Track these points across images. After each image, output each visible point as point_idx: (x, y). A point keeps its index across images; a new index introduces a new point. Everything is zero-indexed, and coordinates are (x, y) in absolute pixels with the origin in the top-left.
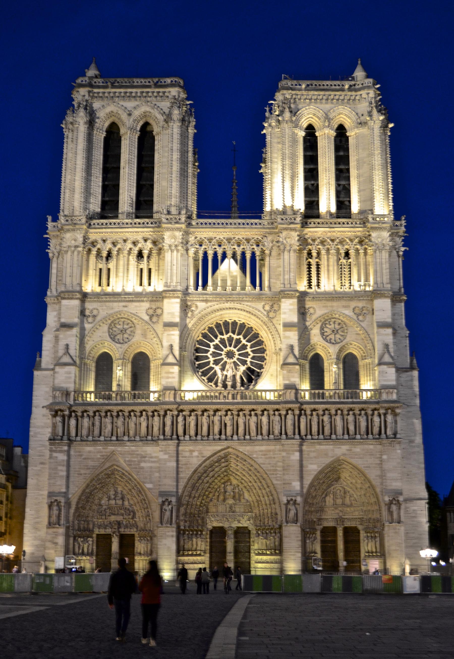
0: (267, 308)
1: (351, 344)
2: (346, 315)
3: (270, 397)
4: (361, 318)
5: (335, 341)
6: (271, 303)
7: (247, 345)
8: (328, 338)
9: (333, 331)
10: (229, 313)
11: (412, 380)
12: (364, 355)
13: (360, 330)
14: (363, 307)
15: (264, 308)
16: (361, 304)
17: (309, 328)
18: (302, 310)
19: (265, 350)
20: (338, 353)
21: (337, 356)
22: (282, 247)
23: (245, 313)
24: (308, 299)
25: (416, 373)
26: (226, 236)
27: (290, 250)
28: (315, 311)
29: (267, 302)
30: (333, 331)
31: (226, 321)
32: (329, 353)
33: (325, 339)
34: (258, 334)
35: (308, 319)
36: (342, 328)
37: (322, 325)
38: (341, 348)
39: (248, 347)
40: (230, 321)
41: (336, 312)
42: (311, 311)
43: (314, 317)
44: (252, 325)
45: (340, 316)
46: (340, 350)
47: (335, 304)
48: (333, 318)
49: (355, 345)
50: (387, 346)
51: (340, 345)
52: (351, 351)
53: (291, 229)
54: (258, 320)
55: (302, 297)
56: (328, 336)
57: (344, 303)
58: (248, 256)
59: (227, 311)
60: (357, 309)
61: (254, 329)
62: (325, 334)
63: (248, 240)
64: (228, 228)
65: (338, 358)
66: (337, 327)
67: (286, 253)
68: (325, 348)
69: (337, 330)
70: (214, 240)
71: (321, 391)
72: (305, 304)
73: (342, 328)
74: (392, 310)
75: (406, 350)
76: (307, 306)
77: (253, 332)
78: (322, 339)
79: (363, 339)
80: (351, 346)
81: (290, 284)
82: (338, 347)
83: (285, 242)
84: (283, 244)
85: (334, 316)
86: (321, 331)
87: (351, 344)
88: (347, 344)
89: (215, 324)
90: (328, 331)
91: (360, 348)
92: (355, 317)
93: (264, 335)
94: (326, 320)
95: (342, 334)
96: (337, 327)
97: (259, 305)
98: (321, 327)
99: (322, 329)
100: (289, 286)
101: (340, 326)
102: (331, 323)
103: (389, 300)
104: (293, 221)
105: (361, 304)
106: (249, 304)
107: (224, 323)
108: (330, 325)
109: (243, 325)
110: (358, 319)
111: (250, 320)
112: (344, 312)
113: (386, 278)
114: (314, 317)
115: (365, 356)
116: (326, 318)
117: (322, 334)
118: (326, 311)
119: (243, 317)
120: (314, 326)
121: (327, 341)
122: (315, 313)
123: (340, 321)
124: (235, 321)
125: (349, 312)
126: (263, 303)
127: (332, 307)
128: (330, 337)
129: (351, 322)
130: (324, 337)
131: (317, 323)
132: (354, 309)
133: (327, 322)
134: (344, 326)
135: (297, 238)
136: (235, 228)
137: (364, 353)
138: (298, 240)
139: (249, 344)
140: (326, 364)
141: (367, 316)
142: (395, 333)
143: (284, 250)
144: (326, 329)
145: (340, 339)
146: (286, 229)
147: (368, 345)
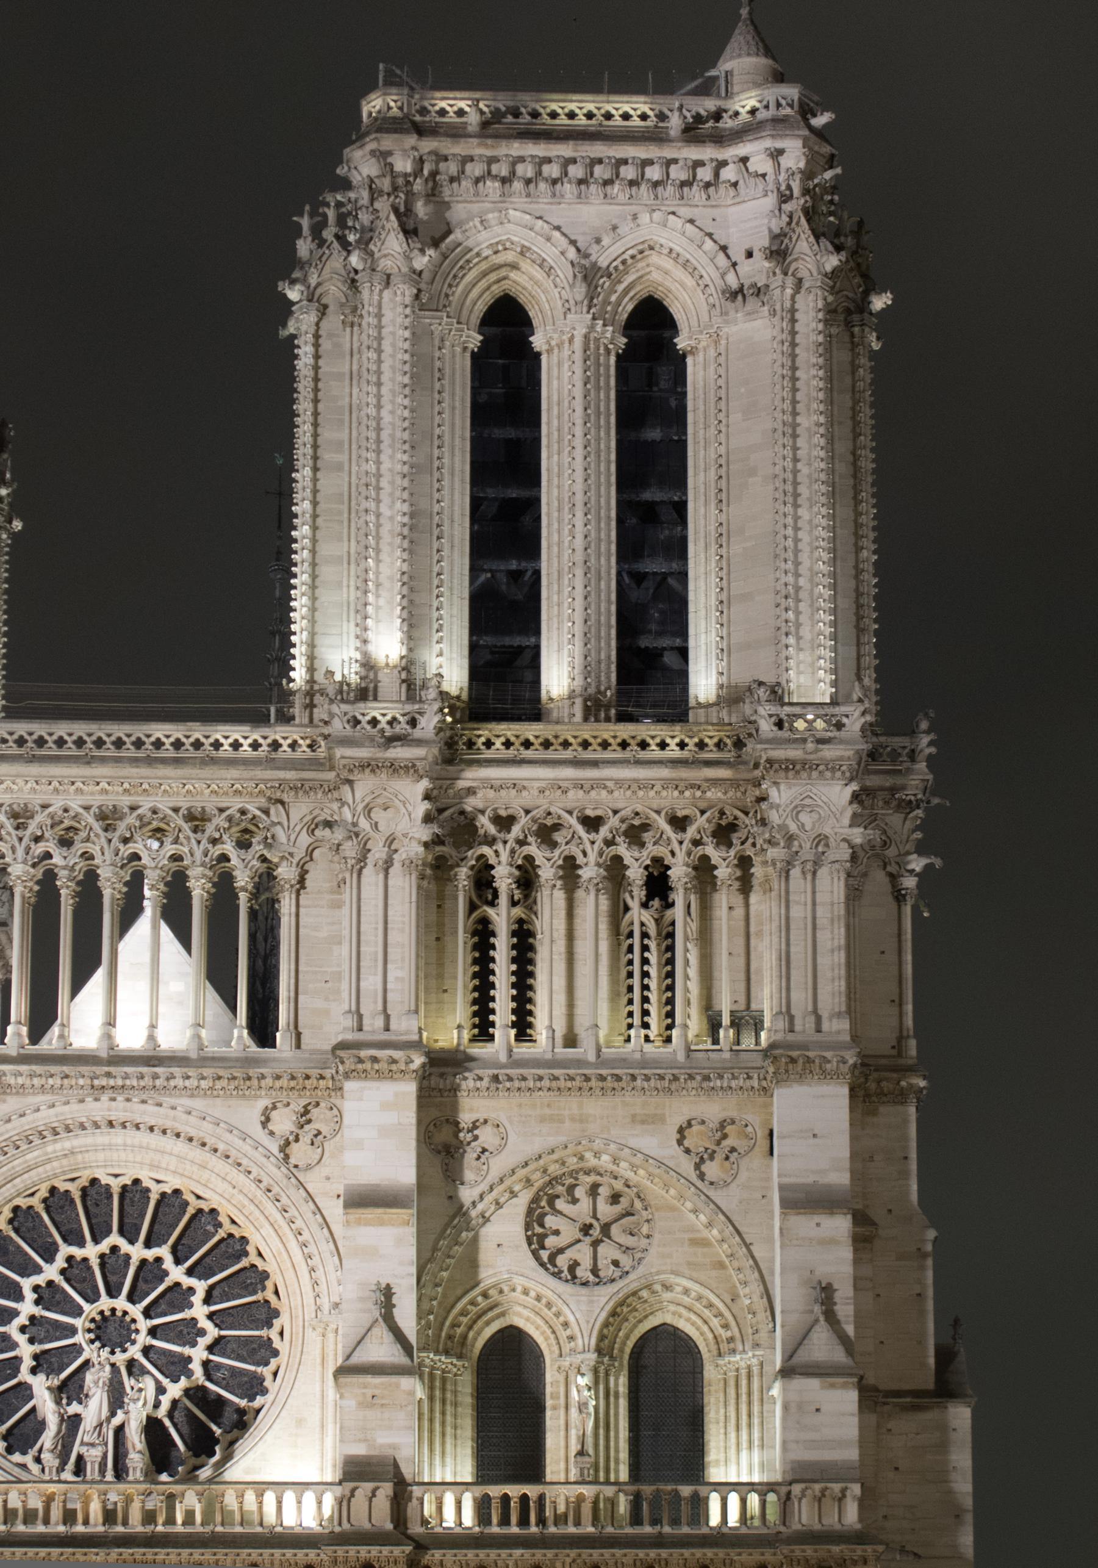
0: (284, 1122)
1: (667, 1287)
2: (647, 1157)
3: (306, 1514)
4: (712, 1169)
5: (595, 1271)
6: (298, 1105)
7: (191, 1290)
8: (562, 1261)
9: (586, 1229)
10: (110, 1147)
11: (943, 1446)
12: (724, 1334)
13: (710, 1225)
14: (722, 1125)
15: (266, 1121)
16: (713, 1109)
17: (473, 1213)
18: (444, 1135)
19: (276, 1314)
20: (606, 1324)
21: (602, 1338)
22: (350, 849)
23: (180, 1146)
24: (471, 1083)
25: (960, 1416)
26: (96, 801)
27: (388, 864)
28: (504, 1138)
29: (283, 1096)
30: (586, 1229)
31: (94, 1181)
32: (565, 1327)
33: (549, 1265)
34: (244, 1240)
35: (469, 1175)
36: (622, 1213)
37: (535, 1200)
38: (622, 1303)
39: (197, 1299)
40: (116, 1185)
41: (598, 1144)
42: (487, 1136)
43: (498, 1165)
44: (213, 1200)
45: (615, 1161)
46: (614, 1314)
47: (594, 1106)
48: (587, 1173)
49: (686, 1292)
50: (826, 1293)
51: (612, 1288)
52: (669, 1319)
53: (395, 768)
54: (241, 1179)
55: (441, 1074)
56: (561, 1251)
57: (635, 1102)
58: (199, 889)
59: (102, 1138)
60: (696, 1128)
61: (223, 1218)
62: (551, 1241)
63: (197, 820)
64: (103, 760)
65: (604, 1348)
66: (606, 1210)
67: (371, 878)
68: (549, 1305)
69: (606, 1229)
70: (40, 818)
71: (532, 1491)
72: (455, 1107)
73: (622, 1213)
74: (854, 1138)
75: (922, 1313)
76: (466, 1118)
77: (221, 1234)
78: (533, 1263)
79: (721, 1265)
80: (667, 1296)
81: (387, 1018)
82: (603, 1299)
83: (364, 824)
84: (354, 833)
85: (591, 1161)
86: (528, 1226)
87: (667, 1287)
88: (649, 1287)
89: (44, 1193)
90: (562, 1227)
91: (710, 1306)
92: (687, 1166)
93: (271, 1244)
94: (553, 1181)
95: (630, 1241)
96: (606, 1210)
97: (248, 1113)
98: (530, 1212)
99: (534, 1218)
100: (380, 1022)
101: (618, 1209)
102: (579, 1192)
103: (845, 1091)
104: (402, 727)
105: (713, 1109)
106: (198, 1104)
107: (84, 1191)
108: (575, 1201)
109: (172, 1201)
110: (702, 1176)
111: (205, 1175)
112: (633, 1142)
113: (832, 994)
114: (498, 1165)
115: (731, 1340)
116: (554, 1169)
117: (536, 1241)
118: (553, 1141)
119: (173, 1163)
120: (499, 1205)
121: (557, 1275)
122: (501, 1148)
123: (618, 1185)
124: (136, 1182)
125: (658, 1143)
126: (264, 1103)
127: (582, 1120)
128: (570, 1254)
129: (666, 1186)
130: (545, 1255)
131: (514, 1195)
132: (681, 1131)
133: (560, 1189)
134: (638, 1205)
135: (422, 808)
136: (135, 761)
137: (726, 1326)
138: (428, 819)
139: (201, 1287)
140: (551, 1376)
141: (744, 1163)
142: (865, 1237)
143: (362, 859)
144: (551, 1221)
145: (616, 1263)
146: (368, 766)
147: (742, 1291)
